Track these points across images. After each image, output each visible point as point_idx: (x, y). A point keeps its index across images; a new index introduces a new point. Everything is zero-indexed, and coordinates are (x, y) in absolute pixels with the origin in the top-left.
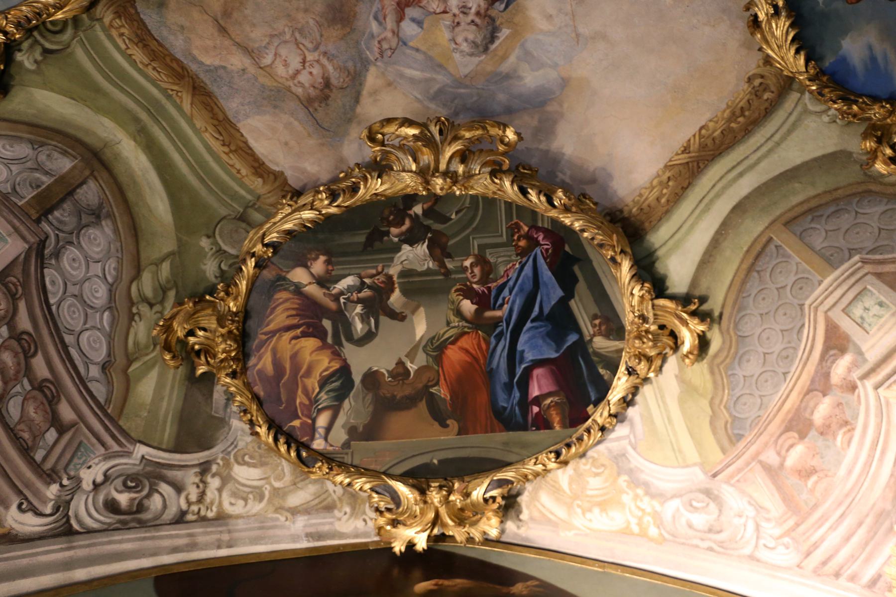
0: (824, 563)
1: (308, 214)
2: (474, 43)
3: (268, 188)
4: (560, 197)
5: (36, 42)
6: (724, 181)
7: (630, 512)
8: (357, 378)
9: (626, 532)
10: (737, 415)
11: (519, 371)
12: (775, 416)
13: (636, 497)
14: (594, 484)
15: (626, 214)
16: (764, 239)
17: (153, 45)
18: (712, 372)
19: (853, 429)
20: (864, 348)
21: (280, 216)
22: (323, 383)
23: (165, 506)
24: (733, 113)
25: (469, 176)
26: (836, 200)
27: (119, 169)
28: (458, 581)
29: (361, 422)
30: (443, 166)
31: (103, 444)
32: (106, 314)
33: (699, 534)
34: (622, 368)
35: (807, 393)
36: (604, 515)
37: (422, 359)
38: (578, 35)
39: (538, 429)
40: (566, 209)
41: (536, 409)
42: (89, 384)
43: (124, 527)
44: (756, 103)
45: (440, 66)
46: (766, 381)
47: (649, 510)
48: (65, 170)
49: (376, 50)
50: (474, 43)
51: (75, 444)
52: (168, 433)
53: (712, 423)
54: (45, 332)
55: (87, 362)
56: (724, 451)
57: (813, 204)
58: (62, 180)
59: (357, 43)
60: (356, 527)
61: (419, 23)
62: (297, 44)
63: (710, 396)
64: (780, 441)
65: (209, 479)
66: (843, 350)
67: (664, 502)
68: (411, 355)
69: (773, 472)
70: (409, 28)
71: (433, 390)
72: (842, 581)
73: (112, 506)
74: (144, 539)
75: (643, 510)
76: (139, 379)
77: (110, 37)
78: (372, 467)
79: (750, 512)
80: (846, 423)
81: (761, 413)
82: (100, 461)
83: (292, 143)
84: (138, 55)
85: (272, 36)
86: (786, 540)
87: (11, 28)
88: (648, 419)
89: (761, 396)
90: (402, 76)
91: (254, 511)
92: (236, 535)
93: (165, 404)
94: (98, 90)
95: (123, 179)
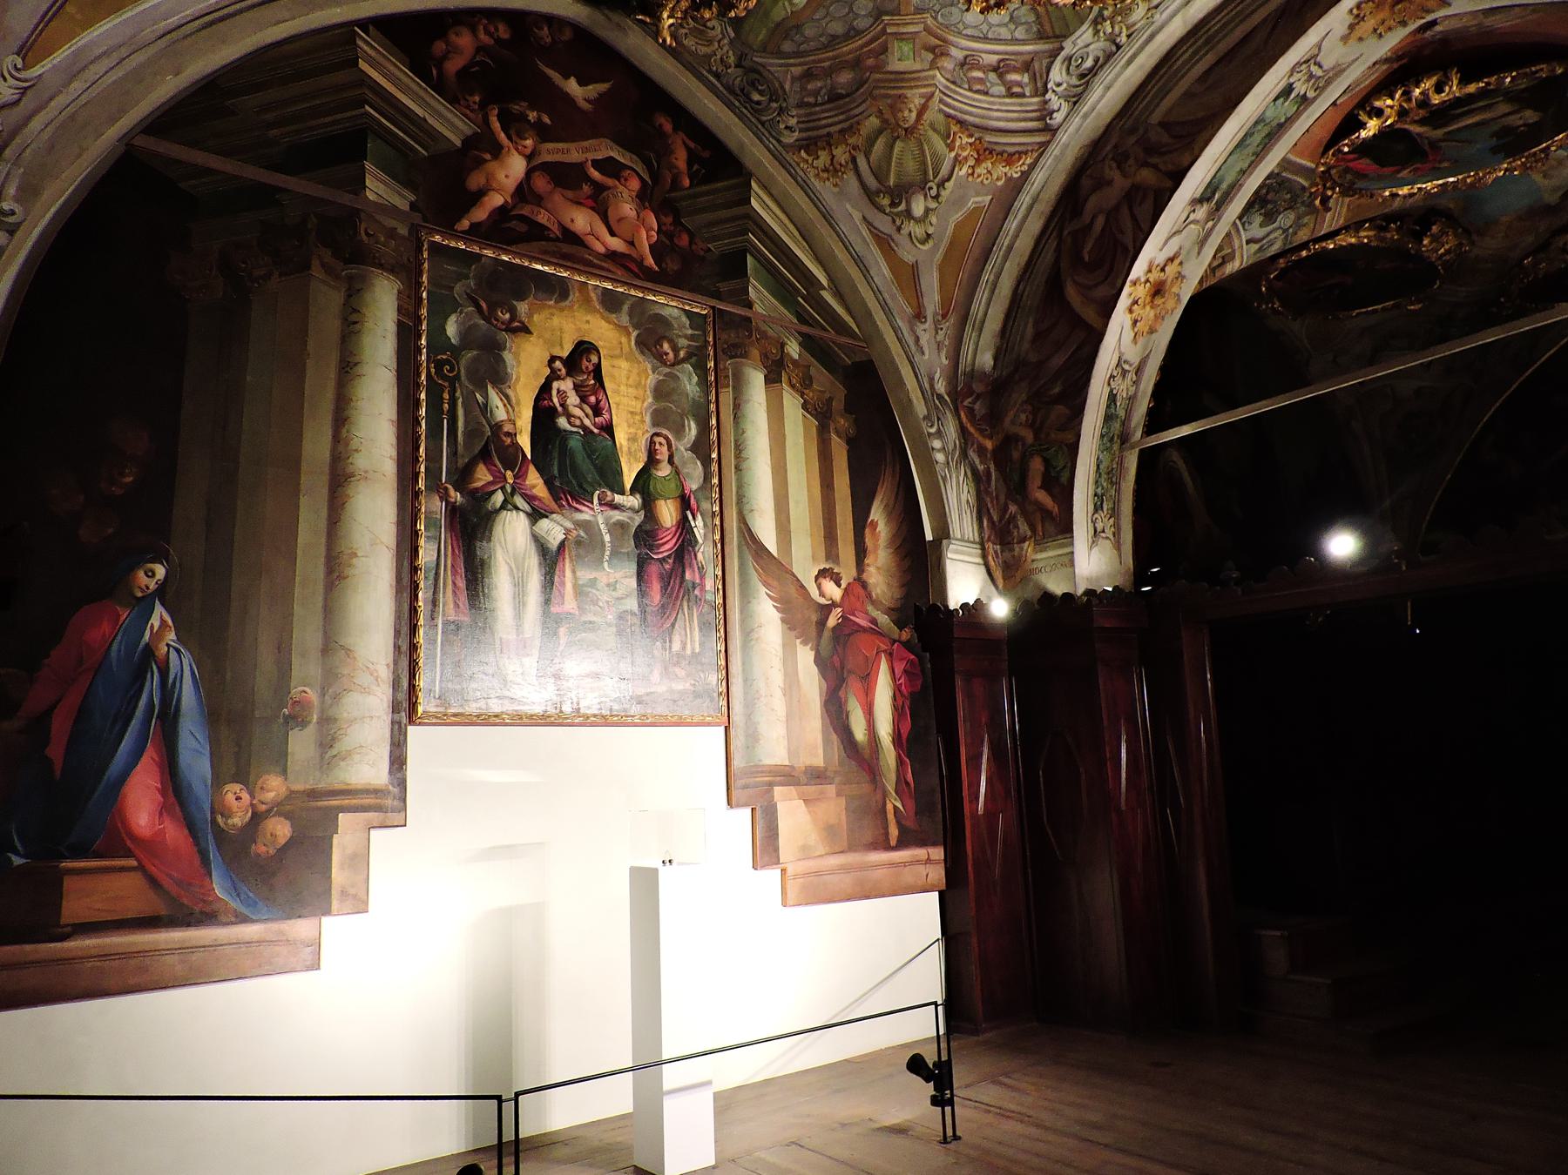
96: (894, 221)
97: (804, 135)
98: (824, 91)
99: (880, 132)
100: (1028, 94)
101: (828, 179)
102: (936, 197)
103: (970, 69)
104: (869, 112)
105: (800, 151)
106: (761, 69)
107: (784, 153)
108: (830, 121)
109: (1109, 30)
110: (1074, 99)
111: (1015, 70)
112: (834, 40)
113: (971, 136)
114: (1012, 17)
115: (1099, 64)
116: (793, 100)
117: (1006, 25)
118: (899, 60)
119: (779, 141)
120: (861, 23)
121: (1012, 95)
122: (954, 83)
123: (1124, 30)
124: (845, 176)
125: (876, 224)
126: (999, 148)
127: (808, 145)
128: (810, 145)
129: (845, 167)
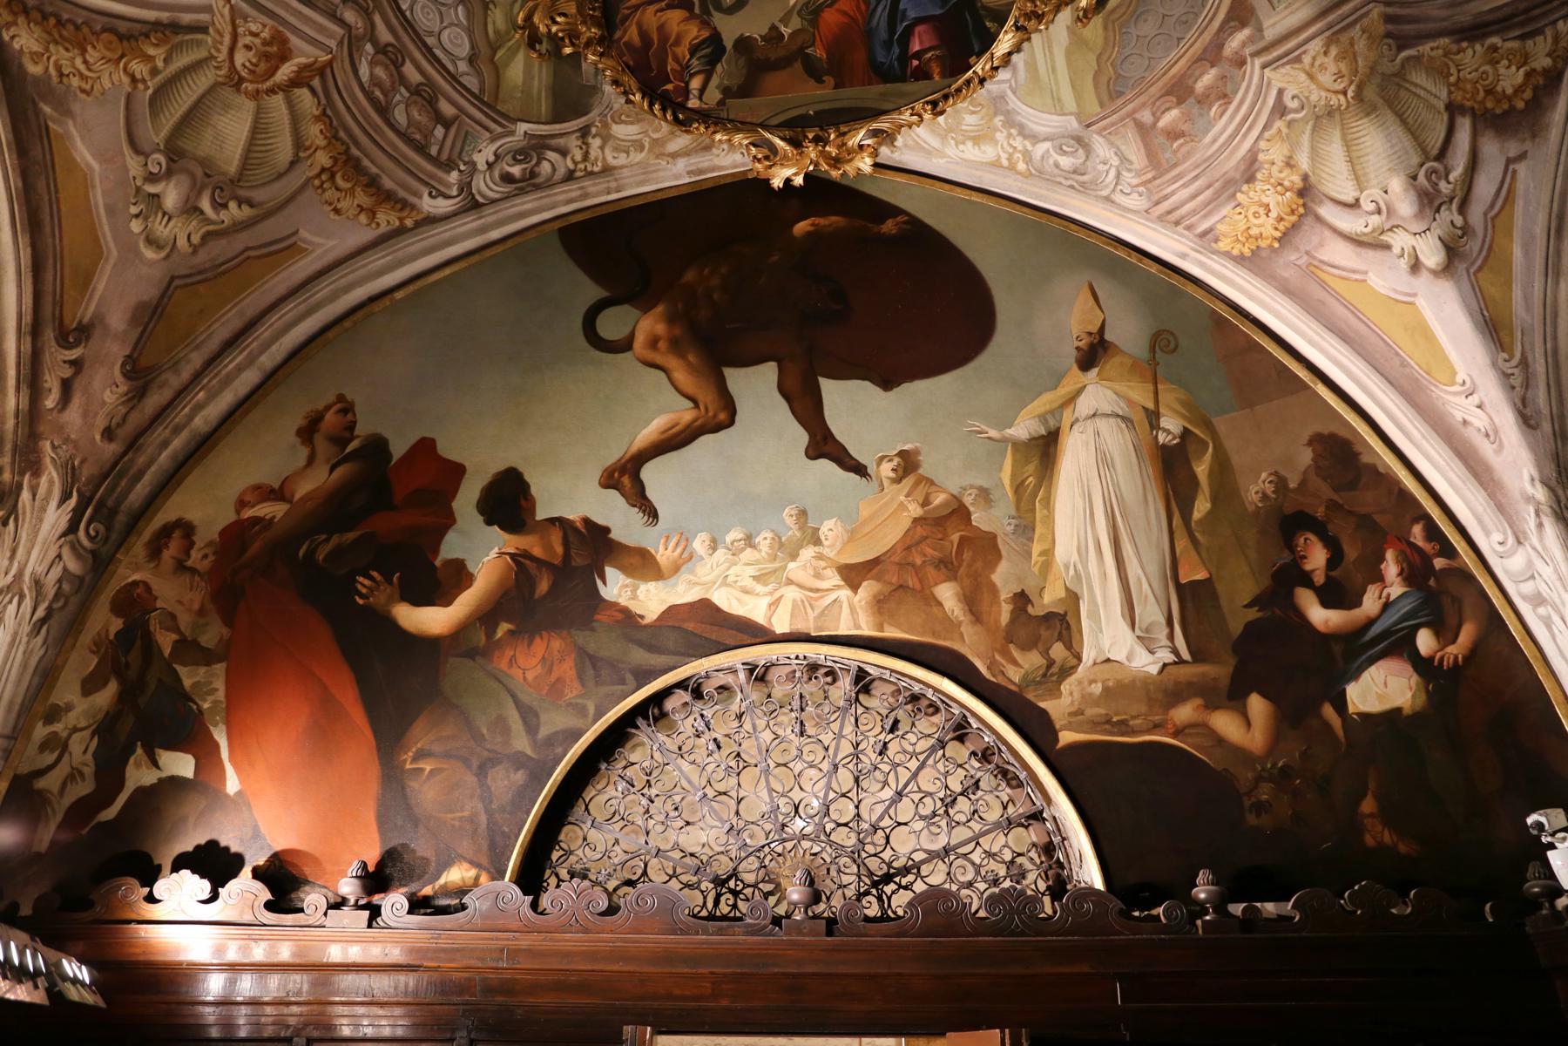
0: (1169, 212)
7: (1002, 148)
8: (729, 44)
9: (996, 164)
10: (1122, 73)
11: (900, 30)
12: (1159, 79)
13: (1010, 136)
14: (970, 119)
18: (1105, 28)
19: (1230, 103)
20: (1265, 25)
22: (694, 50)
23: (554, 169)
28: (834, 218)
29: (734, 82)
31: (487, 129)
32: (460, 8)
33: (1064, 174)
34: (1010, 22)
35: (1195, 62)
36: (977, 148)
37: (796, 23)
39: (917, 79)
41: (916, 63)
42: (461, 79)
43: (522, 192)
46: (1159, 44)
47: (1020, 148)
51: (463, 134)
52: (544, 108)
53: (1095, 78)
54: (406, 40)
55: (454, 59)
56: (1102, 105)
60: (734, 160)
63: (1098, 52)
64: (1158, 104)
65: (590, 140)
66: (1243, 25)
67: (1036, 143)
68: (785, 20)
69: (1144, 131)
71: (808, 51)
72: (1180, 228)
73: (507, 178)
74: (541, 198)
75: (1015, 148)
76: (507, 65)
78: (749, 120)
79: (1115, 161)
80: (1225, 96)
81: (1146, 74)
82: (488, 144)
86: (1141, 189)
88: (1032, 67)
89: (1150, 58)
91: (636, 160)
92: (621, 182)
93: (536, 82)
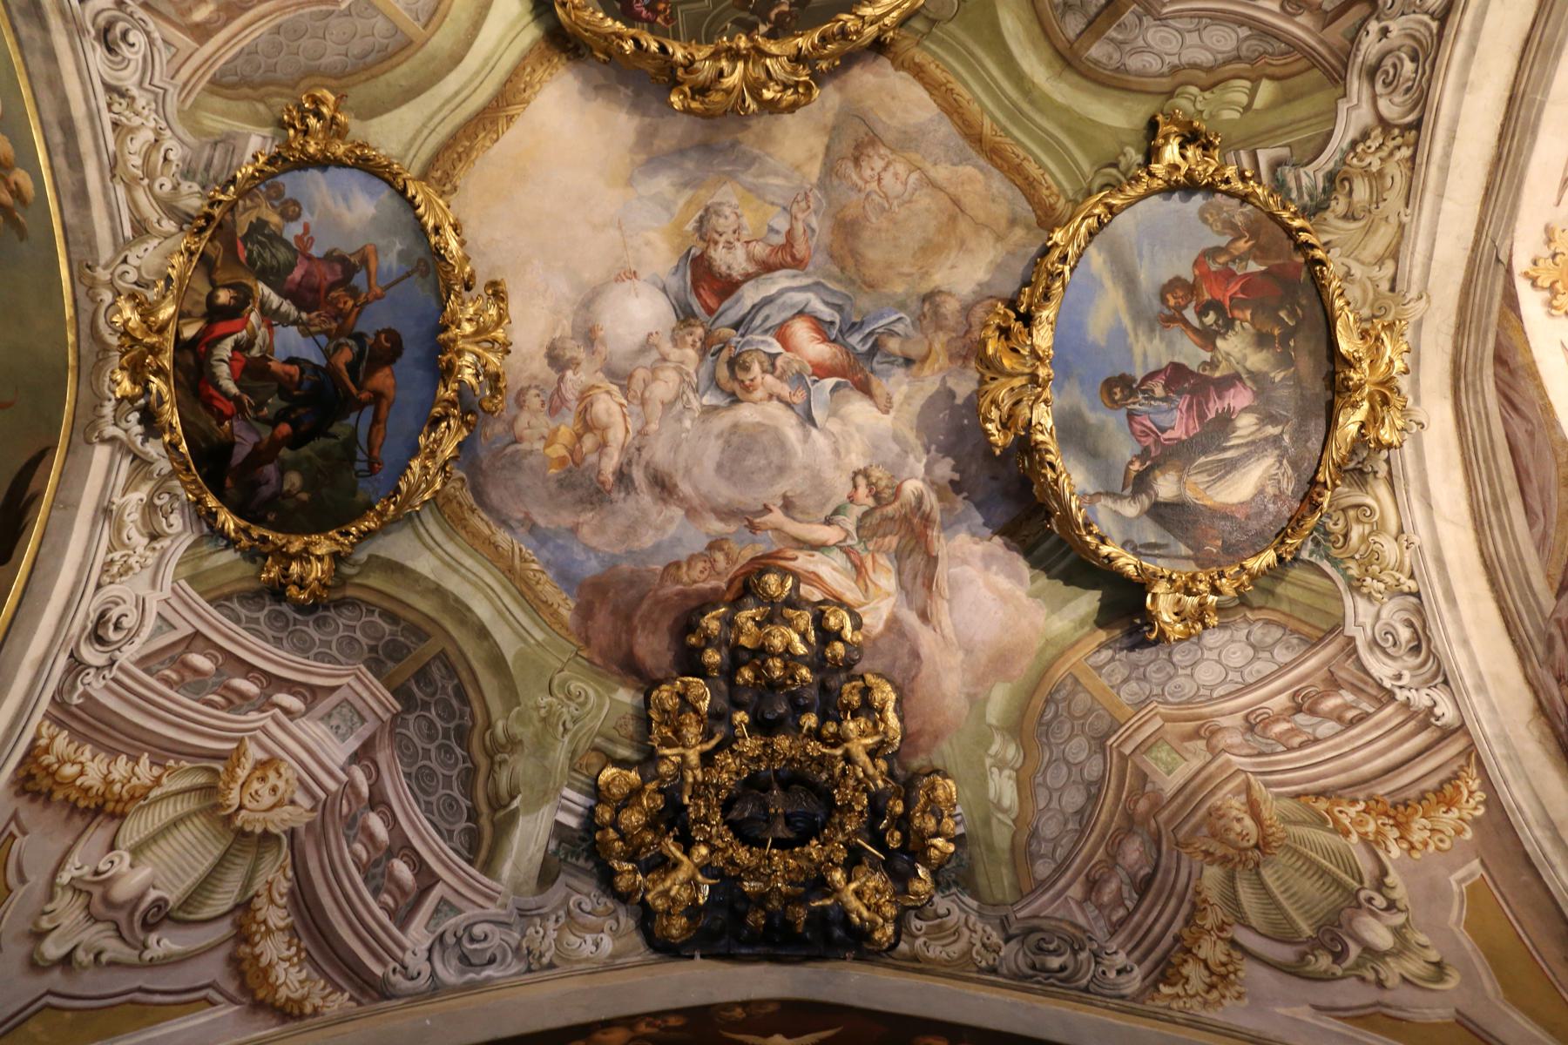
1: (868, 11)
2: (718, 214)
3: (910, 53)
4: (629, 46)
5: (1124, 174)
6: (472, 87)
15: (564, 57)
16: (431, 27)
17: (1019, 180)
21: (895, 14)
24: (468, 155)
25: (715, 56)
26: (367, 68)
27: (1048, 53)
30: (740, 65)
38: (620, 228)
40: (620, 36)
44: (448, 166)
45: (750, 190)
48: (1096, 45)
49: (812, 199)
50: (718, 214)
57: (386, 65)
58: (1099, 35)
59: (830, 204)
61: (772, 230)
62: (886, 197)
70: (782, 224)
77: (1059, 184)
83: (887, 99)
84: (1032, 169)
85: (910, 201)
87: (1146, 178)
90: (786, 177)
94: (1069, 130)
95: (1044, 44)
96: (1363, 979)
97: (1148, 964)
98: (1125, 889)
99: (1231, 878)
100: (1371, 710)
101: (1224, 997)
102: (1391, 906)
103: (1266, 727)
104: (1196, 868)
105: (1158, 990)
106: (1036, 922)
107: (1138, 1006)
108: (1163, 920)
109: (1381, 586)
110: (1440, 679)
111: (1324, 695)
112: (1084, 817)
113: (1354, 802)
114: (1253, 646)
115: (1418, 624)
116: (1100, 932)
117: (1255, 658)
118: (1169, 773)
119: (1123, 997)
120: (1093, 769)
121: (1352, 723)
122: (1260, 754)
123: (1398, 575)
124: (1241, 974)
125: (1342, 1001)
126: (1413, 793)
127: (1163, 973)
128: (1165, 972)
129: (1232, 962)
